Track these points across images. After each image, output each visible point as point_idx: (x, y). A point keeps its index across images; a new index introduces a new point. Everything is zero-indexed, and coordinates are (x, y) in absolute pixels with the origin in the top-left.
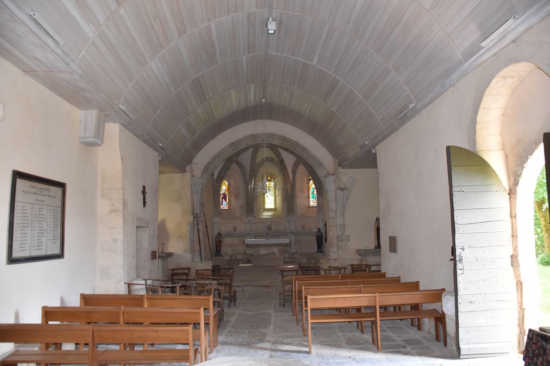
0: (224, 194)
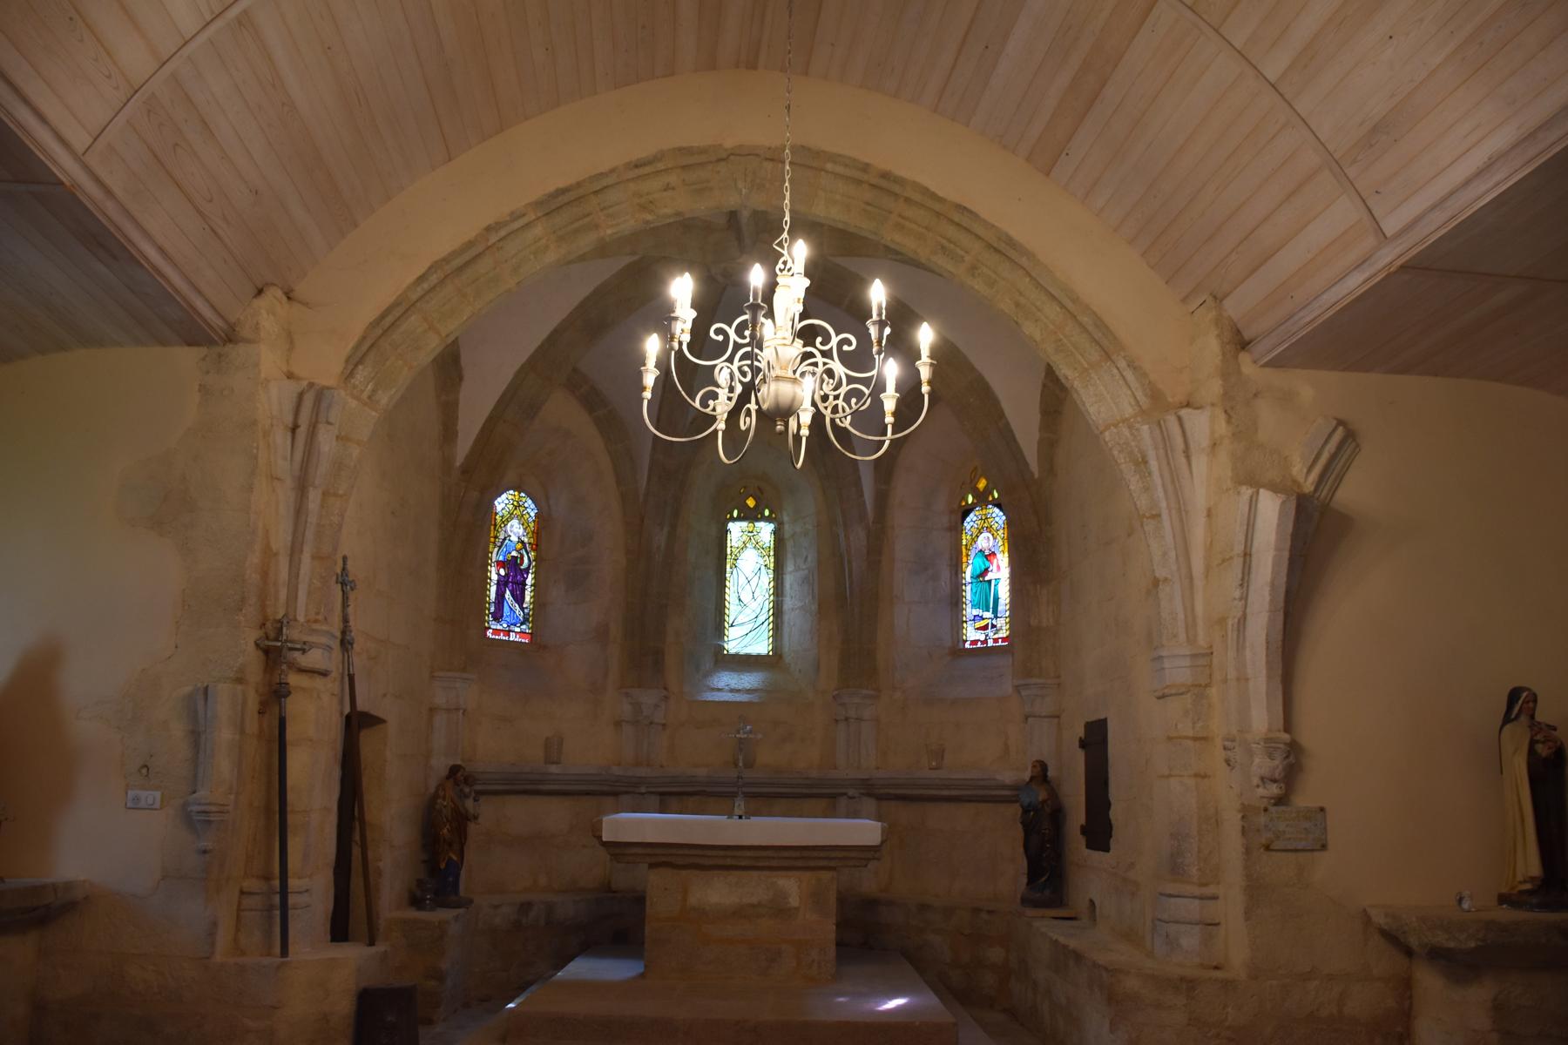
0: (512, 565)
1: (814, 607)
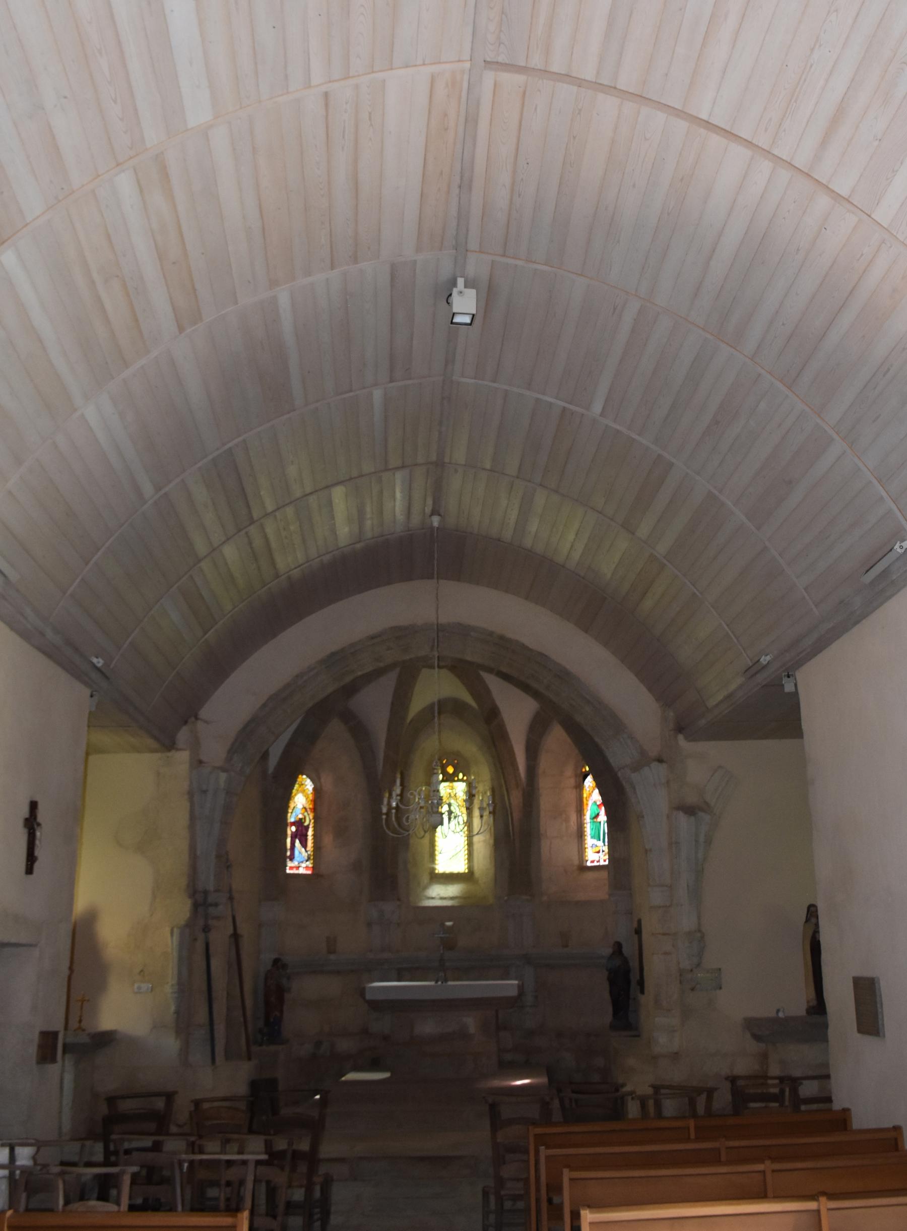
0: (299, 823)
1: (492, 842)
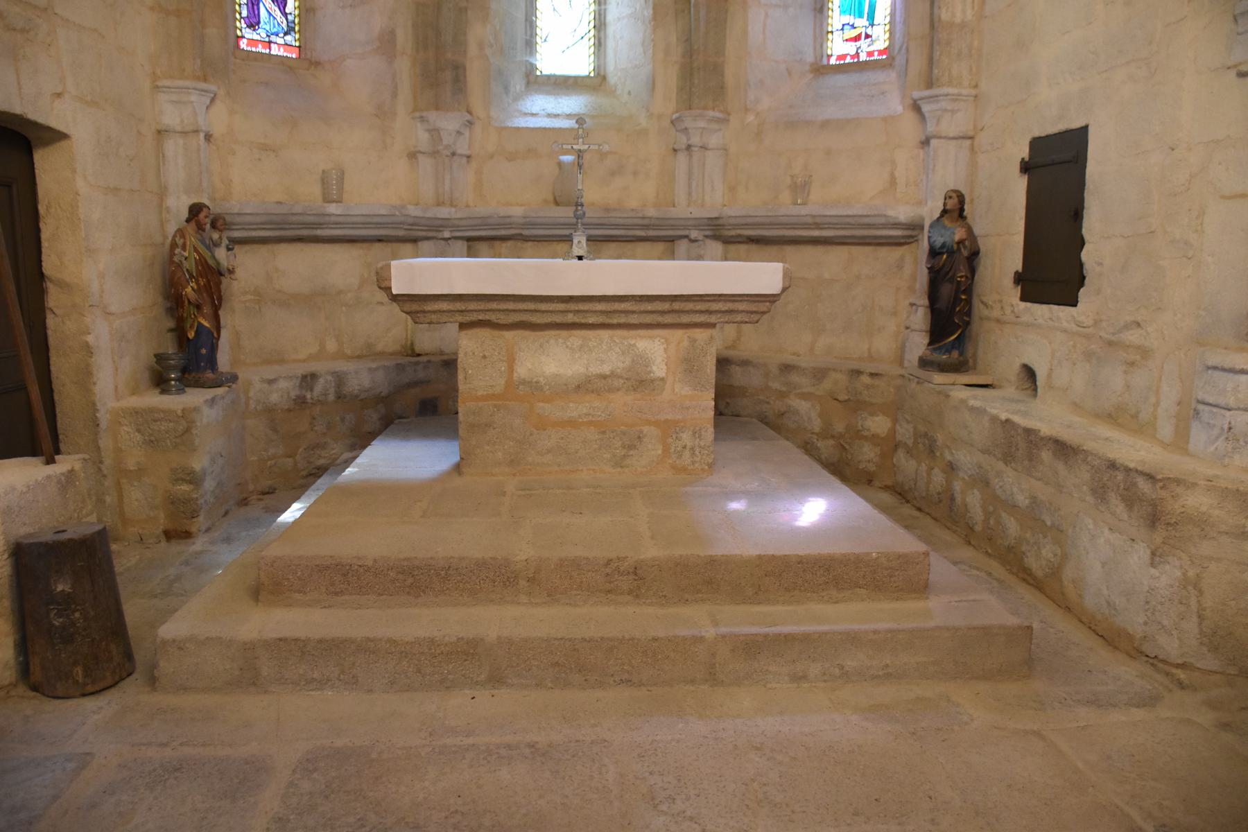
1: (649, 13)
